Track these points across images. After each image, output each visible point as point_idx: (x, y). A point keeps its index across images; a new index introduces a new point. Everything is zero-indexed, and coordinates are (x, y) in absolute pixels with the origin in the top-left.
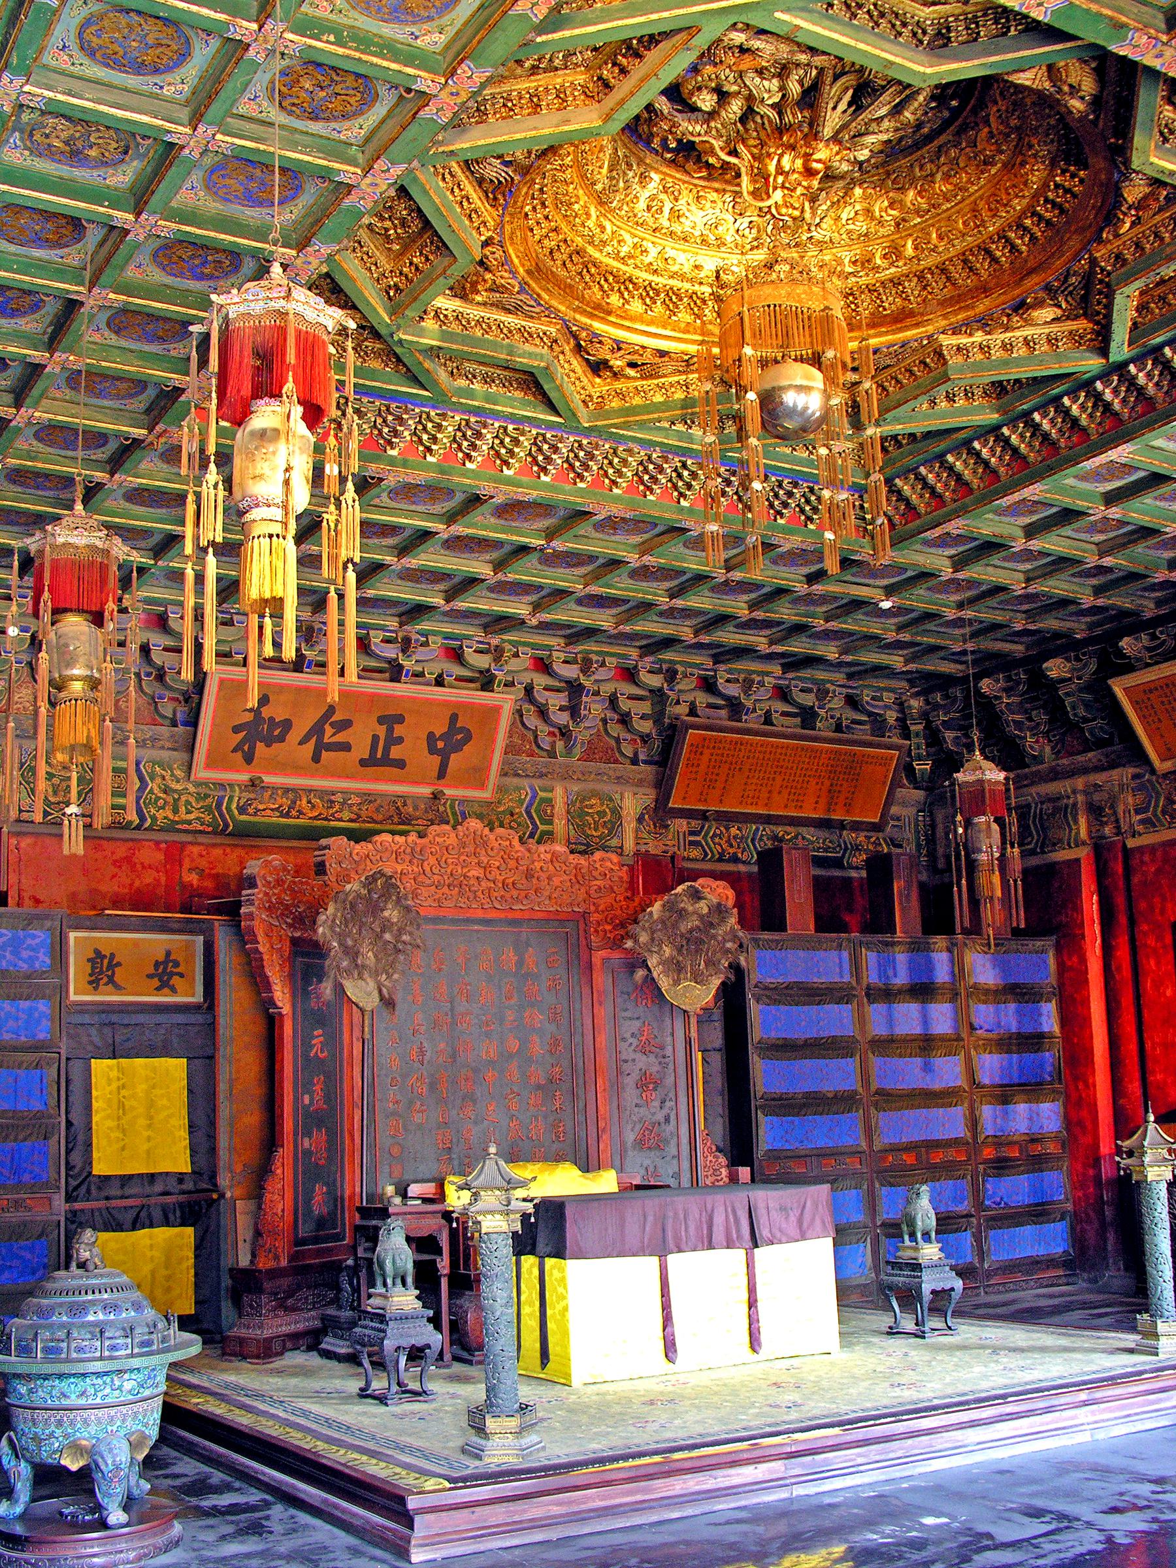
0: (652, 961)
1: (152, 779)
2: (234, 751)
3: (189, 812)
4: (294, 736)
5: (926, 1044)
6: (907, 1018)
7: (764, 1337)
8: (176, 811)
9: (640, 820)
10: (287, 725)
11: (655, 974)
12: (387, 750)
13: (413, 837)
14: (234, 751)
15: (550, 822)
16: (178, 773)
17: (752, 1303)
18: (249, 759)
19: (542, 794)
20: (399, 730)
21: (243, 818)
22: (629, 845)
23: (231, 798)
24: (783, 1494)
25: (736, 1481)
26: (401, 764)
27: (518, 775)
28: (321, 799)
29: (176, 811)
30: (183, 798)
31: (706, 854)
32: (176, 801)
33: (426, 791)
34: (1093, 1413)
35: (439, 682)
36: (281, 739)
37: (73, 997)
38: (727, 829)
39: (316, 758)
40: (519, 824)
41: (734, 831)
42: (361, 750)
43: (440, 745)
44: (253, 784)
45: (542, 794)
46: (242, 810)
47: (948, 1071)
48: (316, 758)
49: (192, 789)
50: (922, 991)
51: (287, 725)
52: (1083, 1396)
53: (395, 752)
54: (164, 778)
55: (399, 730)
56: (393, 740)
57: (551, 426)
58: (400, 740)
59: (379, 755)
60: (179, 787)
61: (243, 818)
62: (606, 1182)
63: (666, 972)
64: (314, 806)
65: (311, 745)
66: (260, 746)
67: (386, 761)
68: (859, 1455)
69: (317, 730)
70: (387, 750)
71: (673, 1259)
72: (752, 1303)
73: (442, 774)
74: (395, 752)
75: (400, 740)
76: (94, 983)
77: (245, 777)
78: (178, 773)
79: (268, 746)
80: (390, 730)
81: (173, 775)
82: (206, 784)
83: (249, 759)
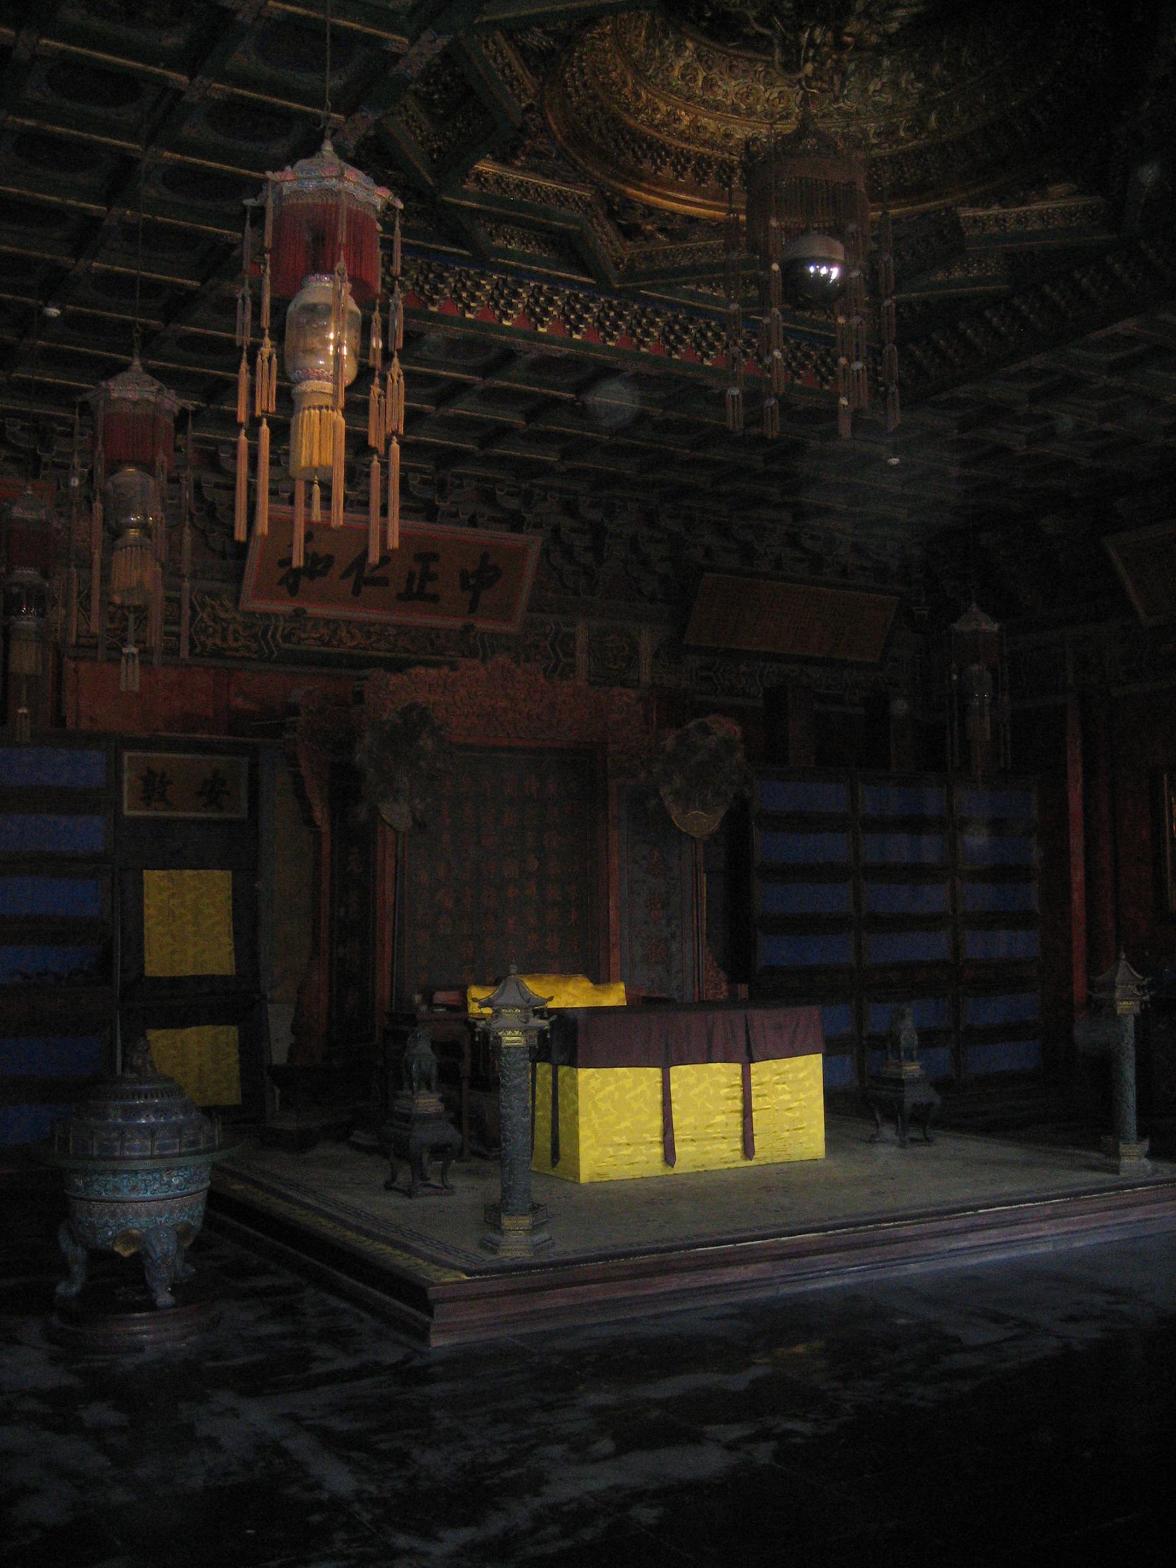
0: (664, 791)
1: (203, 609)
2: (280, 583)
3: (236, 640)
4: (336, 570)
5: (917, 873)
6: (898, 848)
8: (224, 639)
9: (656, 655)
11: (666, 804)
13: (445, 669)
14: (280, 583)
15: (572, 656)
16: (227, 603)
17: (747, 1112)
18: (293, 590)
19: (566, 630)
21: (287, 646)
22: (646, 678)
23: (276, 628)
24: (769, 1293)
25: (727, 1280)
26: (434, 598)
29: (224, 639)
30: (231, 627)
32: (225, 629)
33: (458, 624)
35: (472, 522)
37: (127, 812)
39: (356, 591)
41: (743, 668)
43: (472, 582)
44: (298, 614)
45: (566, 630)
46: (286, 638)
47: (933, 898)
49: (239, 618)
50: (914, 824)
52: (1048, 1211)
53: (430, 588)
54: (213, 608)
55: (433, 568)
57: (583, 286)
59: (415, 589)
61: (287, 646)
62: (615, 997)
64: (353, 637)
65: (351, 579)
71: (676, 1072)
72: (747, 1112)
73: (472, 610)
74: (430, 588)
76: (147, 799)
77: (285, 607)
78: (227, 603)
81: (222, 605)
82: (253, 613)
83: (293, 590)
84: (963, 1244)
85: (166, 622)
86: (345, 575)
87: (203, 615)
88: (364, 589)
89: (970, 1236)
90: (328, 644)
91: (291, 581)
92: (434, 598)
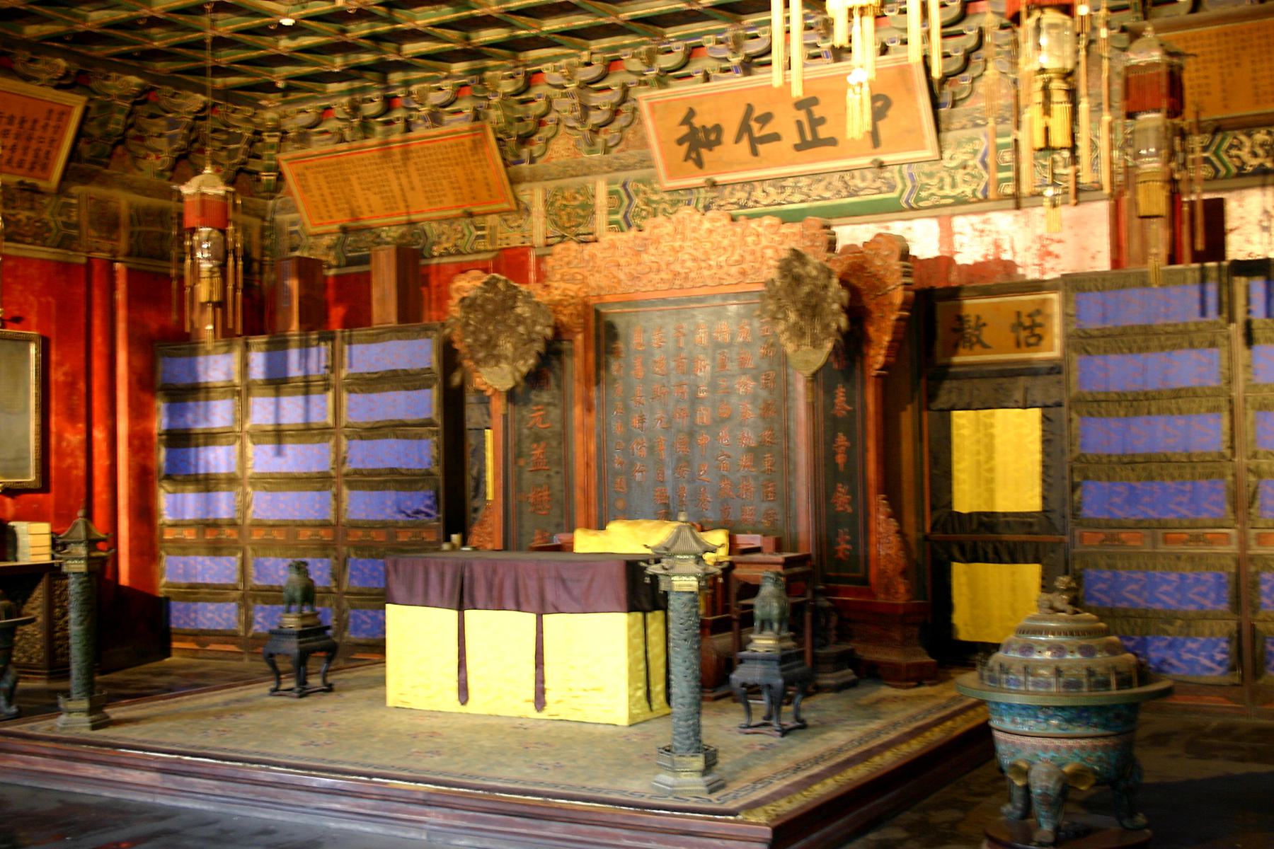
2: (687, 158)
7: (548, 697)
10: (718, 129)
12: (814, 132)
18: (699, 163)
20: (818, 112)
25: (128, 779)
26: (832, 142)
27: (977, 125)
28: (774, 186)
31: (1217, 171)
33: (866, 161)
34: (446, 816)
36: (718, 142)
38: (1249, 136)
39: (755, 153)
40: (973, 176)
42: (791, 137)
48: (755, 153)
51: (718, 129)
53: (823, 132)
55: (818, 112)
56: (816, 122)
58: (822, 121)
59: (809, 137)
60: (655, 198)
63: (789, 339)
64: (768, 194)
65: (745, 142)
66: (704, 152)
67: (817, 142)
68: (218, 788)
69: (745, 128)
70: (814, 132)
74: (823, 132)
75: (822, 121)
79: (711, 150)
80: (810, 114)
83: (699, 163)
84: (338, 806)
85: (610, 213)
86: (737, 141)
87: (636, 201)
88: (761, 148)
89: (344, 799)
90: (745, 207)
91: (694, 155)
92: (832, 142)
